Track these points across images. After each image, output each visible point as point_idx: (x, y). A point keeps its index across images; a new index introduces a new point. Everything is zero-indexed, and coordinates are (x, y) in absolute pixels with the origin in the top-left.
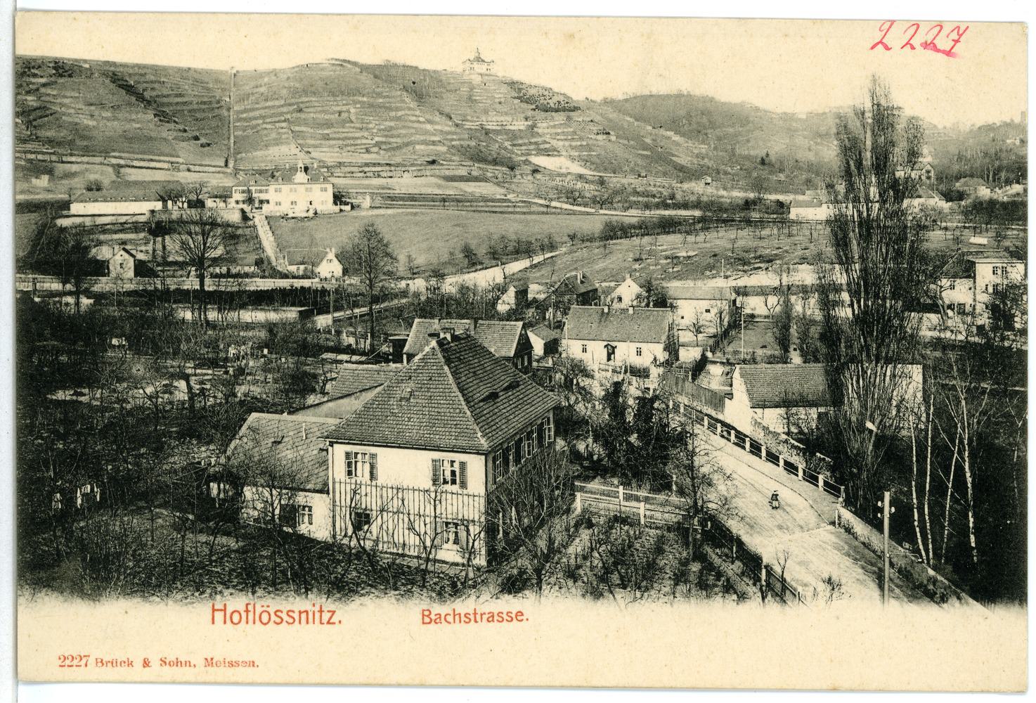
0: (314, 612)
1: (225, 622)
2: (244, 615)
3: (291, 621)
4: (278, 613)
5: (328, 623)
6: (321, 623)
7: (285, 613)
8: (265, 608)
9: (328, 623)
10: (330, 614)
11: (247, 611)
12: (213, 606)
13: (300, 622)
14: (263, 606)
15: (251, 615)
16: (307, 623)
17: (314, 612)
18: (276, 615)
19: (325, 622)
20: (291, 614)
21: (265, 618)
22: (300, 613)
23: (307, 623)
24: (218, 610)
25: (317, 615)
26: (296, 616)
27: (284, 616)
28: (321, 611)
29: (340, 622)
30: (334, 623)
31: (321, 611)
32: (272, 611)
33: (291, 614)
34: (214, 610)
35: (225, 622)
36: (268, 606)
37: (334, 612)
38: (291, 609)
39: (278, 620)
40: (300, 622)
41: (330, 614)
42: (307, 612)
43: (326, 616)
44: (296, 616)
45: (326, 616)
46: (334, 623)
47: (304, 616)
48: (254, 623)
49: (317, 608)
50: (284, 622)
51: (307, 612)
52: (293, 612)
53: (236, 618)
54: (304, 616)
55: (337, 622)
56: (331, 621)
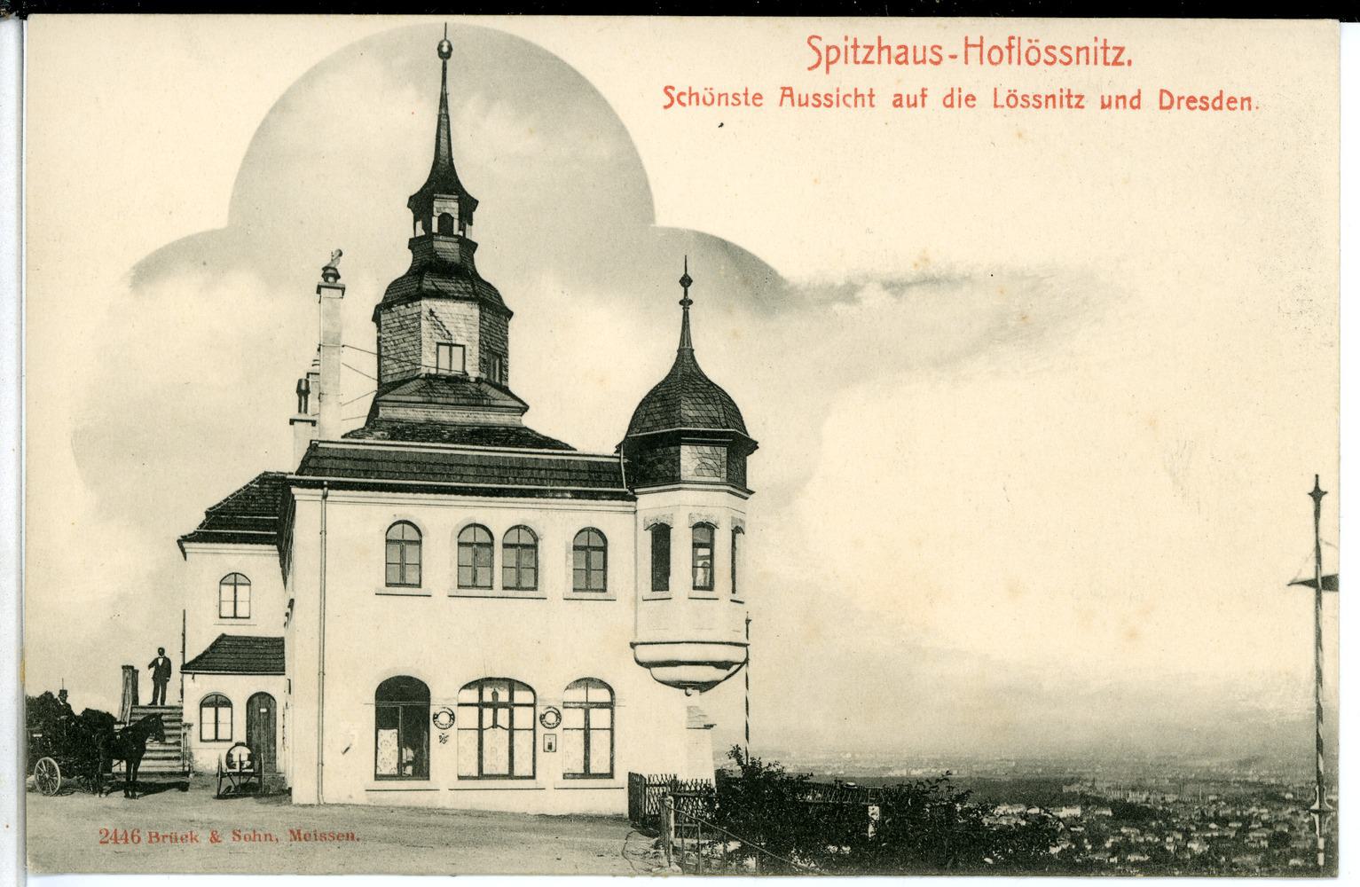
0: (1096, 48)
1: (982, 63)
2: (1006, 52)
4: (1050, 50)
6: (1106, 63)
7: (1058, 49)
8: (1034, 44)
9: (1113, 64)
11: (1010, 47)
12: (966, 39)
14: (1030, 41)
15: (1015, 51)
16: (1088, 62)
17: (1096, 48)
19: (1110, 59)
20: (1066, 50)
21: (1033, 55)
22: (1079, 49)
23: (1088, 62)
24: (975, 46)
25: (1101, 53)
26: (1073, 53)
27: (1057, 53)
28: (1105, 48)
29: (1130, 63)
30: (1122, 64)
31: (1105, 48)
33: (1066, 50)
34: (967, 46)
35: (982, 63)
36: (1037, 41)
37: (1121, 50)
39: (1050, 59)
41: (1117, 51)
42: (1087, 48)
43: (1111, 55)
44: (1073, 53)
46: (1122, 64)
47: (1083, 54)
48: (1019, 63)
49: (1100, 44)
51: (1087, 48)
52: (1070, 48)
53: (996, 55)
54: (1083, 54)
55: (1126, 63)
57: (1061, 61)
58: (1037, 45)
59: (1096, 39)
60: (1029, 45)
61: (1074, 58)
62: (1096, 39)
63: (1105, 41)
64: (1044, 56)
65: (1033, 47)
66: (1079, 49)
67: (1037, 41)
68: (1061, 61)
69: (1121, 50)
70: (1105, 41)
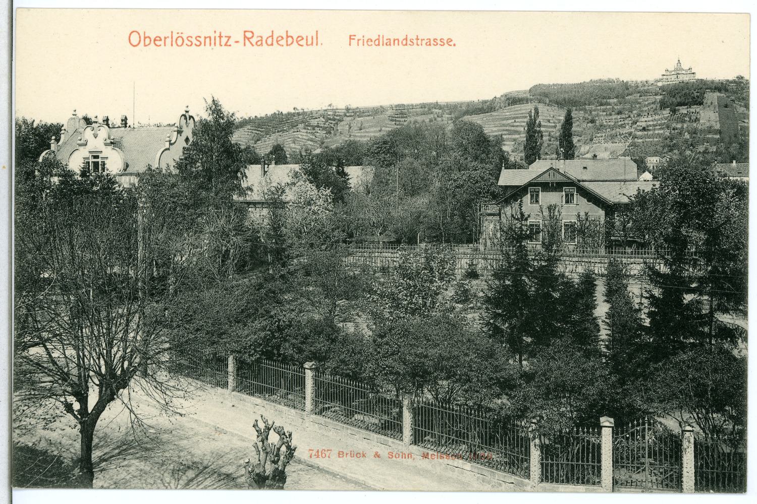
0: (215, 37)
3: (198, 43)
4: (190, 39)
5: (226, 45)
6: (221, 45)
7: (194, 38)
9: (226, 45)
10: (227, 39)
13: (205, 45)
14: (178, 33)
17: (215, 37)
18: (188, 40)
19: (223, 43)
20: (198, 38)
21: (180, 42)
22: (205, 38)
25: (218, 39)
26: (202, 40)
27: (195, 41)
28: (220, 37)
31: (220, 37)
32: (185, 36)
36: (182, 33)
37: (229, 37)
38: (199, 35)
39: (190, 43)
40: (205, 45)
42: (210, 38)
43: (224, 40)
44: (202, 40)
45: (224, 40)
47: (208, 40)
49: (217, 35)
50: (194, 45)
54: (208, 40)
56: (228, 44)
57: (196, 45)
58: (181, 35)
59: (215, 32)
60: (178, 35)
61: (203, 44)
62: (215, 32)
63: (220, 33)
64: (186, 41)
65: (181, 37)
66: (205, 38)
67: (182, 33)
68: (196, 45)
69: (229, 37)
70: (220, 33)
